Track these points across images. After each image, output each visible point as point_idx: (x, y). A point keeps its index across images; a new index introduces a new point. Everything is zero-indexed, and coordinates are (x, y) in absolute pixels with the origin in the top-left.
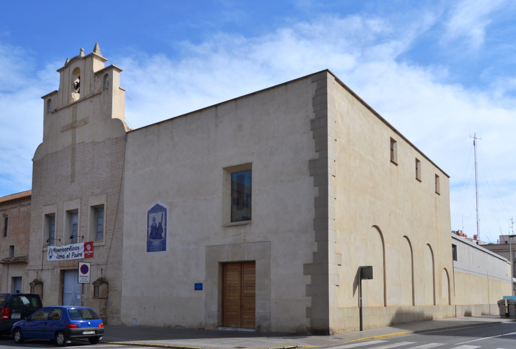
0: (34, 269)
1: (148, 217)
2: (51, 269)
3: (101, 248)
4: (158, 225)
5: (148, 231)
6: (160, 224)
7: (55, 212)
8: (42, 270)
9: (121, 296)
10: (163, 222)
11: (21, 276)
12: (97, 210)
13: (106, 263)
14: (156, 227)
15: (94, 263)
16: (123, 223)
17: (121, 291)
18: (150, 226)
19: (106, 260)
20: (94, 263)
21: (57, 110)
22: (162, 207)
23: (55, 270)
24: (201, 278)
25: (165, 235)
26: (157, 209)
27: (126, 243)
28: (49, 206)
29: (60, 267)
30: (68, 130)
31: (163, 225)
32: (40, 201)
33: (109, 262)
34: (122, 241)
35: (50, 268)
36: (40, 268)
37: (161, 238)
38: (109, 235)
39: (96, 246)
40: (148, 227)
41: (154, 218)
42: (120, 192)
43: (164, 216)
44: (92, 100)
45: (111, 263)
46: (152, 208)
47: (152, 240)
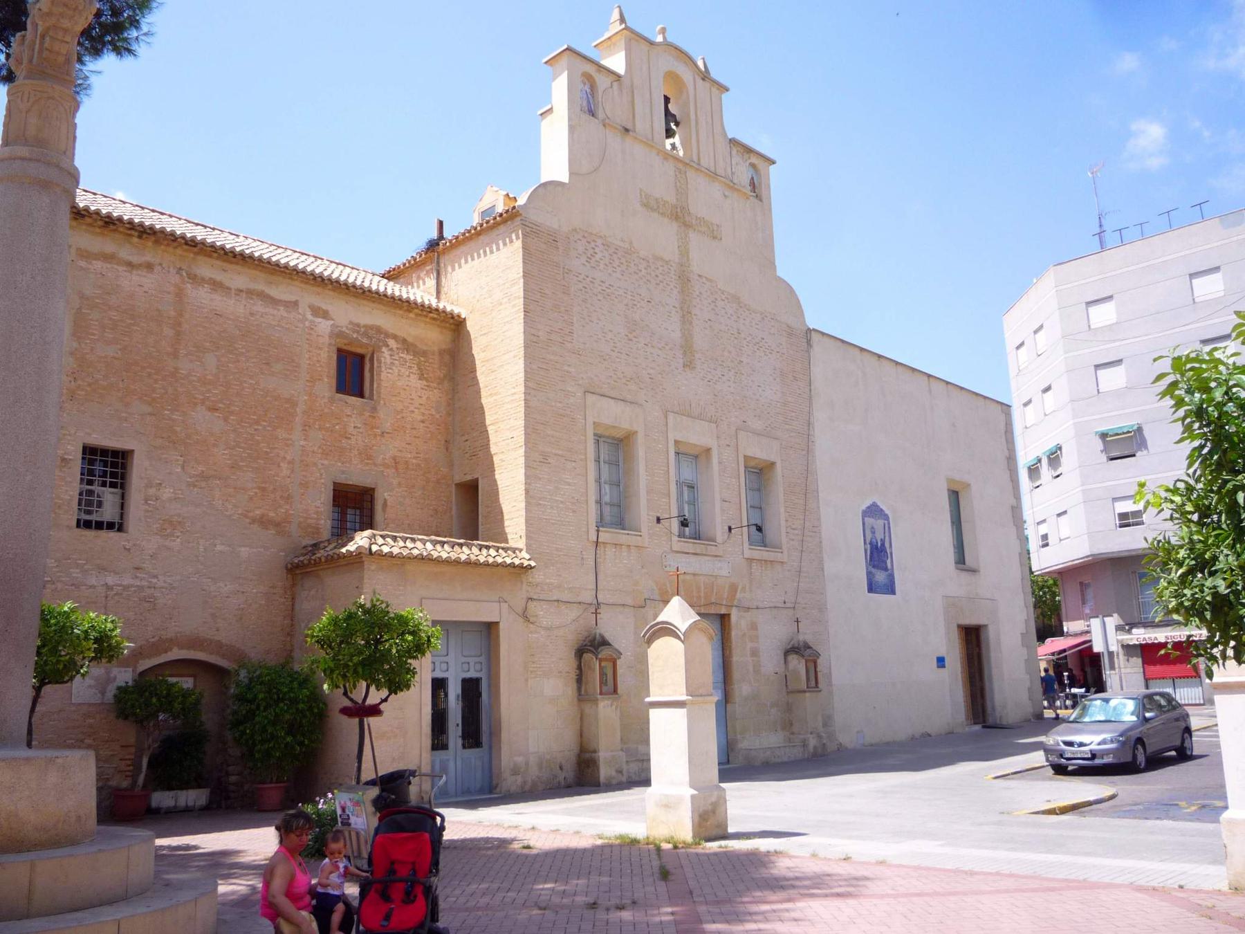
0: (555, 598)
1: (864, 524)
2: (634, 607)
4: (879, 545)
5: (866, 551)
6: (883, 541)
7: (635, 428)
9: (831, 685)
10: (887, 539)
12: (759, 474)
13: (792, 606)
14: (877, 546)
16: (819, 519)
18: (868, 542)
22: (882, 510)
24: (942, 652)
25: (892, 565)
26: (874, 511)
31: (887, 545)
32: (566, 368)
34: (821, 562)
35: (630, 601)
36: (588, 597)
37: (886, 569)
38: (793, 540)
39: (766, 561)
40: (865, 543)
41: (873, 528)
42: (808, 450)
43: (887, 528)
44: (727, 193)
45: (804, 608)
46: (868, 508)
47: (873, 570)
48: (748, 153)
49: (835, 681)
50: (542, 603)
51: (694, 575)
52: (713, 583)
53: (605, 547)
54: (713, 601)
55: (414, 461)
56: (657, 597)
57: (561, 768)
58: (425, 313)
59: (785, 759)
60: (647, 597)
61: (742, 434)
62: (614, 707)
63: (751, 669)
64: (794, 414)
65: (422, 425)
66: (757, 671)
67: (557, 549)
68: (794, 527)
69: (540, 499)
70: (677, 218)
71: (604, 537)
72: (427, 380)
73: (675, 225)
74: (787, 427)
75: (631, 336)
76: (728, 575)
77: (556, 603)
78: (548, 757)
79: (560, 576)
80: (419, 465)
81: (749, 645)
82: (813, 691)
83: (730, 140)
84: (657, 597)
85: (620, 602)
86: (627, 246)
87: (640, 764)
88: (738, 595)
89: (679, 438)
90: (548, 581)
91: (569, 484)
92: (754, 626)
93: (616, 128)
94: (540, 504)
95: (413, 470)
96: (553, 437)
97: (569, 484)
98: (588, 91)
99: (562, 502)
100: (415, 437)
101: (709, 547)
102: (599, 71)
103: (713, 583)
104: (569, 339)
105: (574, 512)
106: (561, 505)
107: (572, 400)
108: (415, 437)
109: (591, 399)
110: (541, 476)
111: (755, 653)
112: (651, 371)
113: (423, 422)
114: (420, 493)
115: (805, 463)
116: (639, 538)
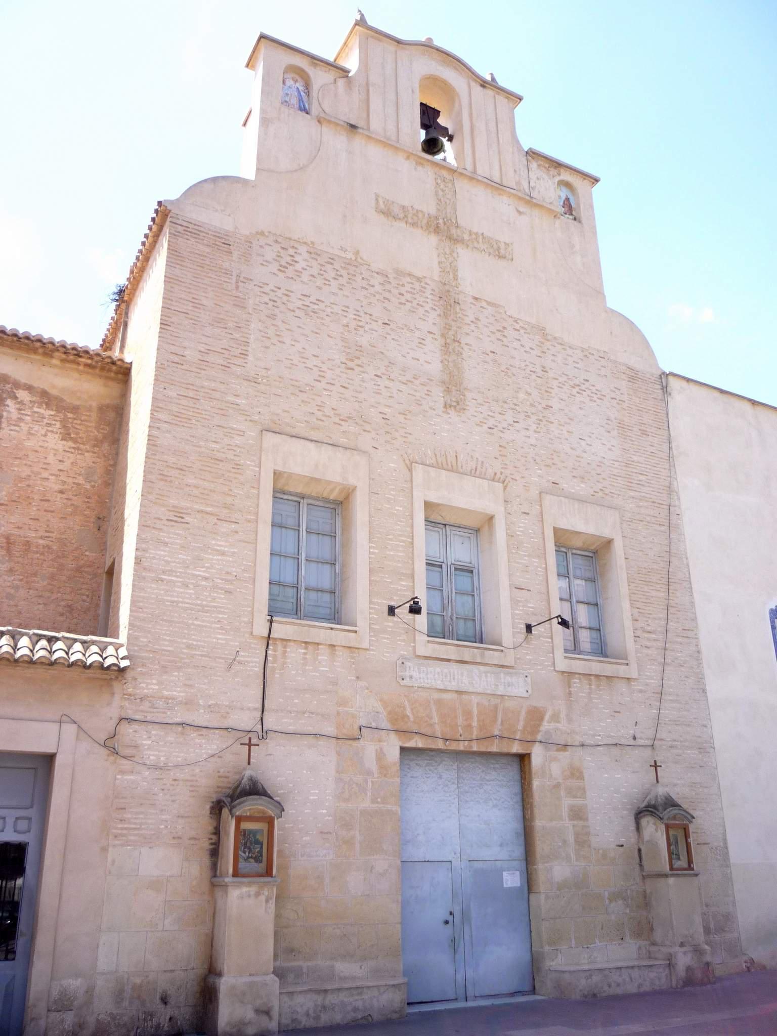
0: (178, 720)
3: (622, 687)
8: (264, 734)
9: (728, 866)
11: (50, 750)
13: (649, 743)
15: (594, 735)
16: (694, 619)
17: (727, 848)
19: (650, 733)
20: (594, 735)
21: (360, 130)
23: (369, 748)
27: (715, 687)
28: (311, 446)
29: (401, 732)
30: (414, 224)
32: (231, 398)
33: (661, 740)
34: (700, 679)
35: (330, 730)
36: (246, 720)
39: (597, 676)
44: (521, 209)
48: (556, 167)
49: (735, 855)
50: (150, 727)
51: (460, 693)
52: (496, 707)
53: (285, 647)
54: (496, 733)
55: (41, 542)
56: (385, 724)
57: (164, 1001)
58: (71, 357)
59: (632, 989)
60: (363, 722)
61: (548, 500)
62: (263, 898)
63: (571, 839)
64: (641, 477)
65: (59, 495)
66: (582, 840)
67: (189, 647)
68: (649, 629)
69: (164, 572)
70: (437, 230)
71: (283, 629)
72: (75, 441)
73: (433, 239)
74: (633, 494)
75: (350, 364)
76: (525, 695)
77: (180, 729)
78: (138, 981)
79: (191, 686)
80: (49, 547)
81: (567, 802)
82: (684, 875)
83: (527, 153)
84: (385, 724)
85: (310, 729)
86: (350, 255)
87: (319, 999)
88: (546, 726)
89: (433, 498)
90: (166, 693)
91: (223, 554)
92: (576, 773)
93: (337, 124)
94: (162, 580)
95: (37, 552)
96: (196, 487)
97: (223, 554)
98: (301, 88)
99: (206, 579)
100: (45, 511)
101: (487, 652)
102: (315, 65)
103: (496, 707)
104: (239, 361)
105: (229, 592)
106: (204, 583)
107: (238, 440)
108: (45, 511)
109: (270, 440)
110: (166, 540)
111: (578, 814)
112: (386, 410)
113: (61, 492)
114: (45, 583)
115: (667, 542)
116: (353, 634)
